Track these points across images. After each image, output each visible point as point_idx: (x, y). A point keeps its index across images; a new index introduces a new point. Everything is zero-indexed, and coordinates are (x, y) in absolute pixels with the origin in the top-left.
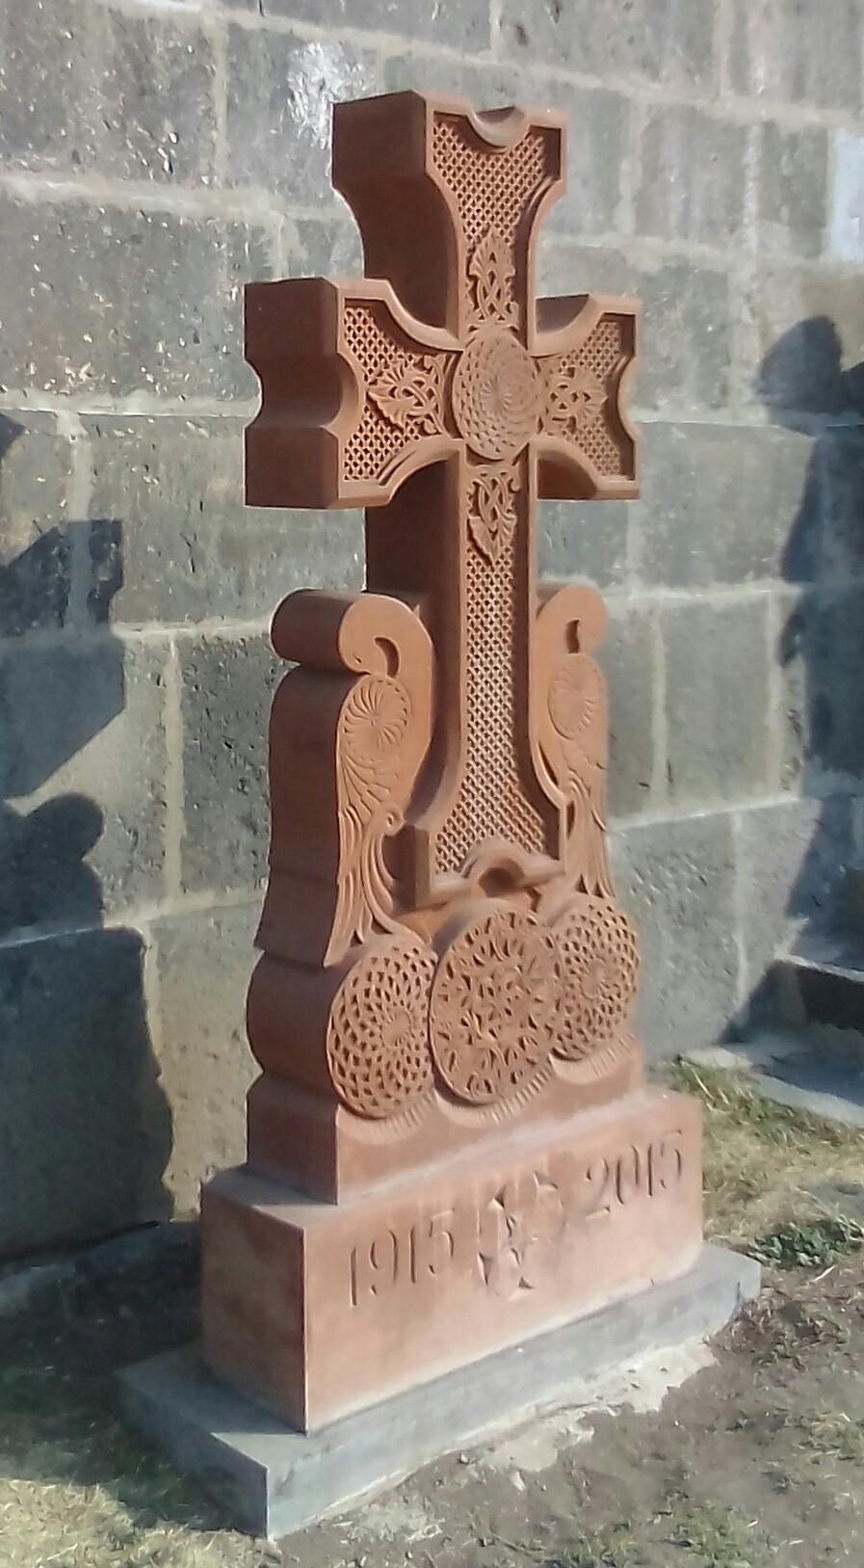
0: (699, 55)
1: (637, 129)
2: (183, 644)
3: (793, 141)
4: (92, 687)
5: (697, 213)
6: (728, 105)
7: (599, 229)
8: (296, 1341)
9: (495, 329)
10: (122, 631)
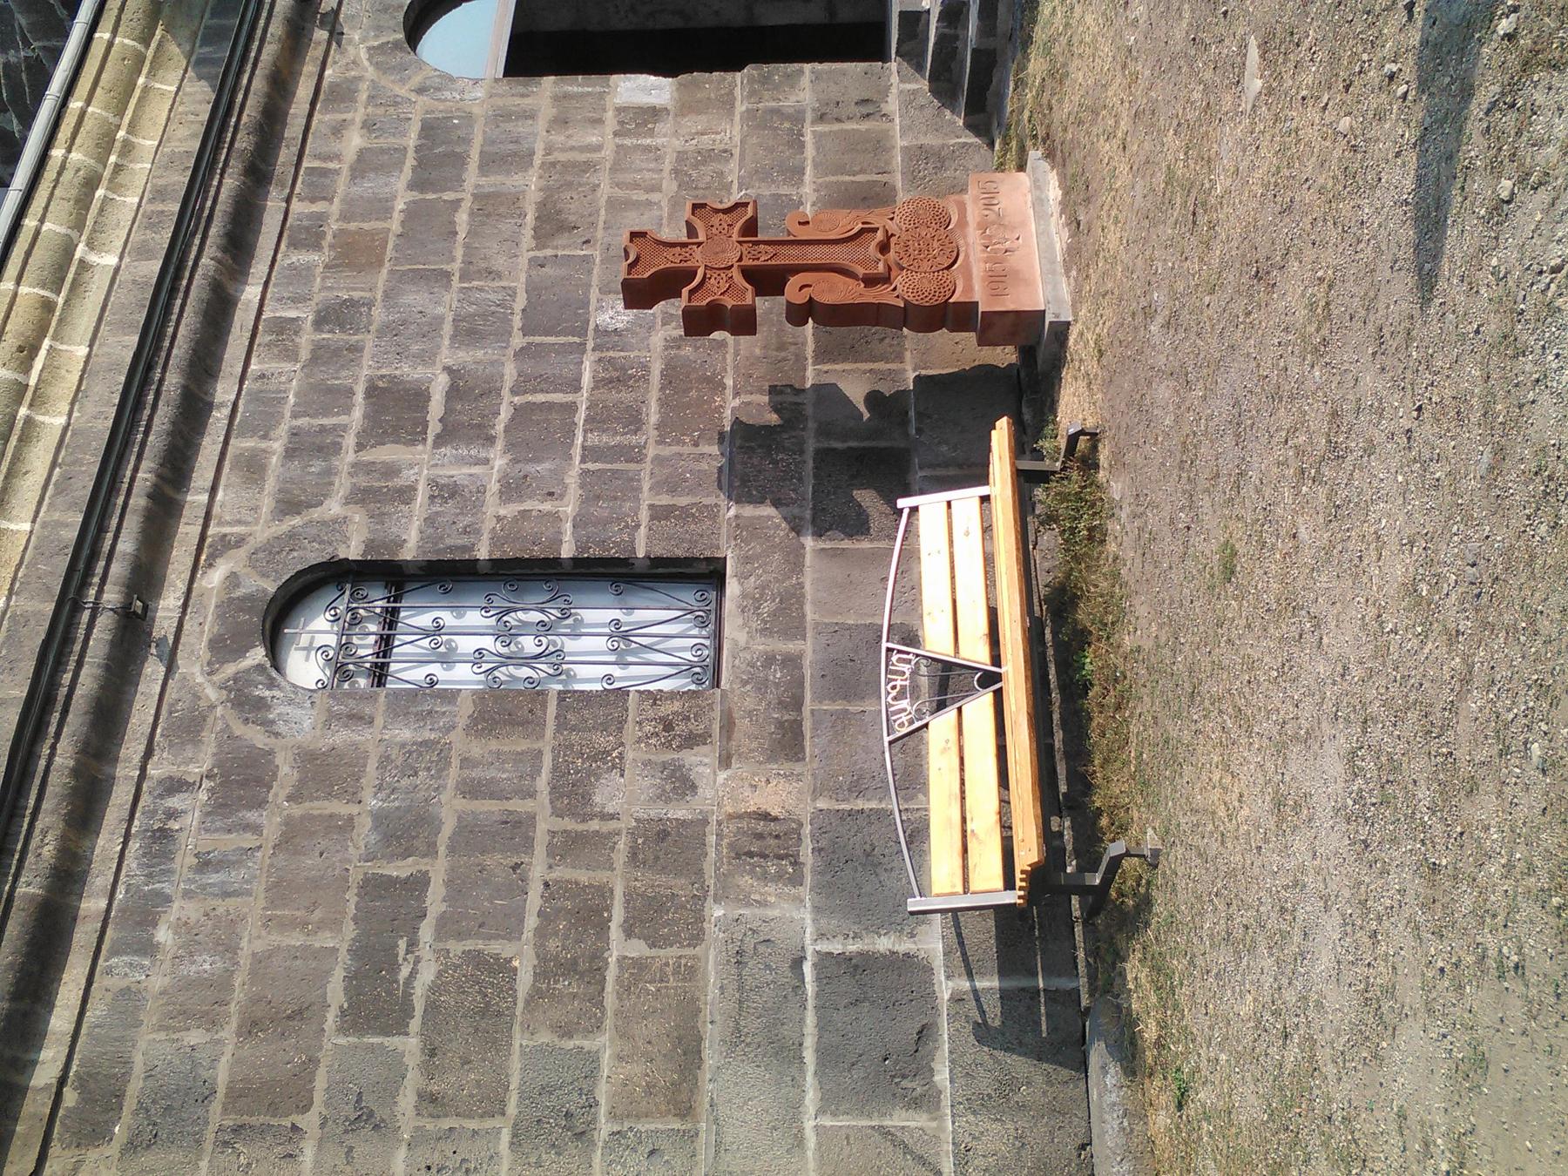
0: (589, 166)
1: (619, 193)
2: (814, 364)
3: (621, 123)
4: (828, 394)
5: (652, 166)
6: (608, 153)
7: (660, 208)
8: (1018, 314)
9: (698, 252)
10: (808, 385)
